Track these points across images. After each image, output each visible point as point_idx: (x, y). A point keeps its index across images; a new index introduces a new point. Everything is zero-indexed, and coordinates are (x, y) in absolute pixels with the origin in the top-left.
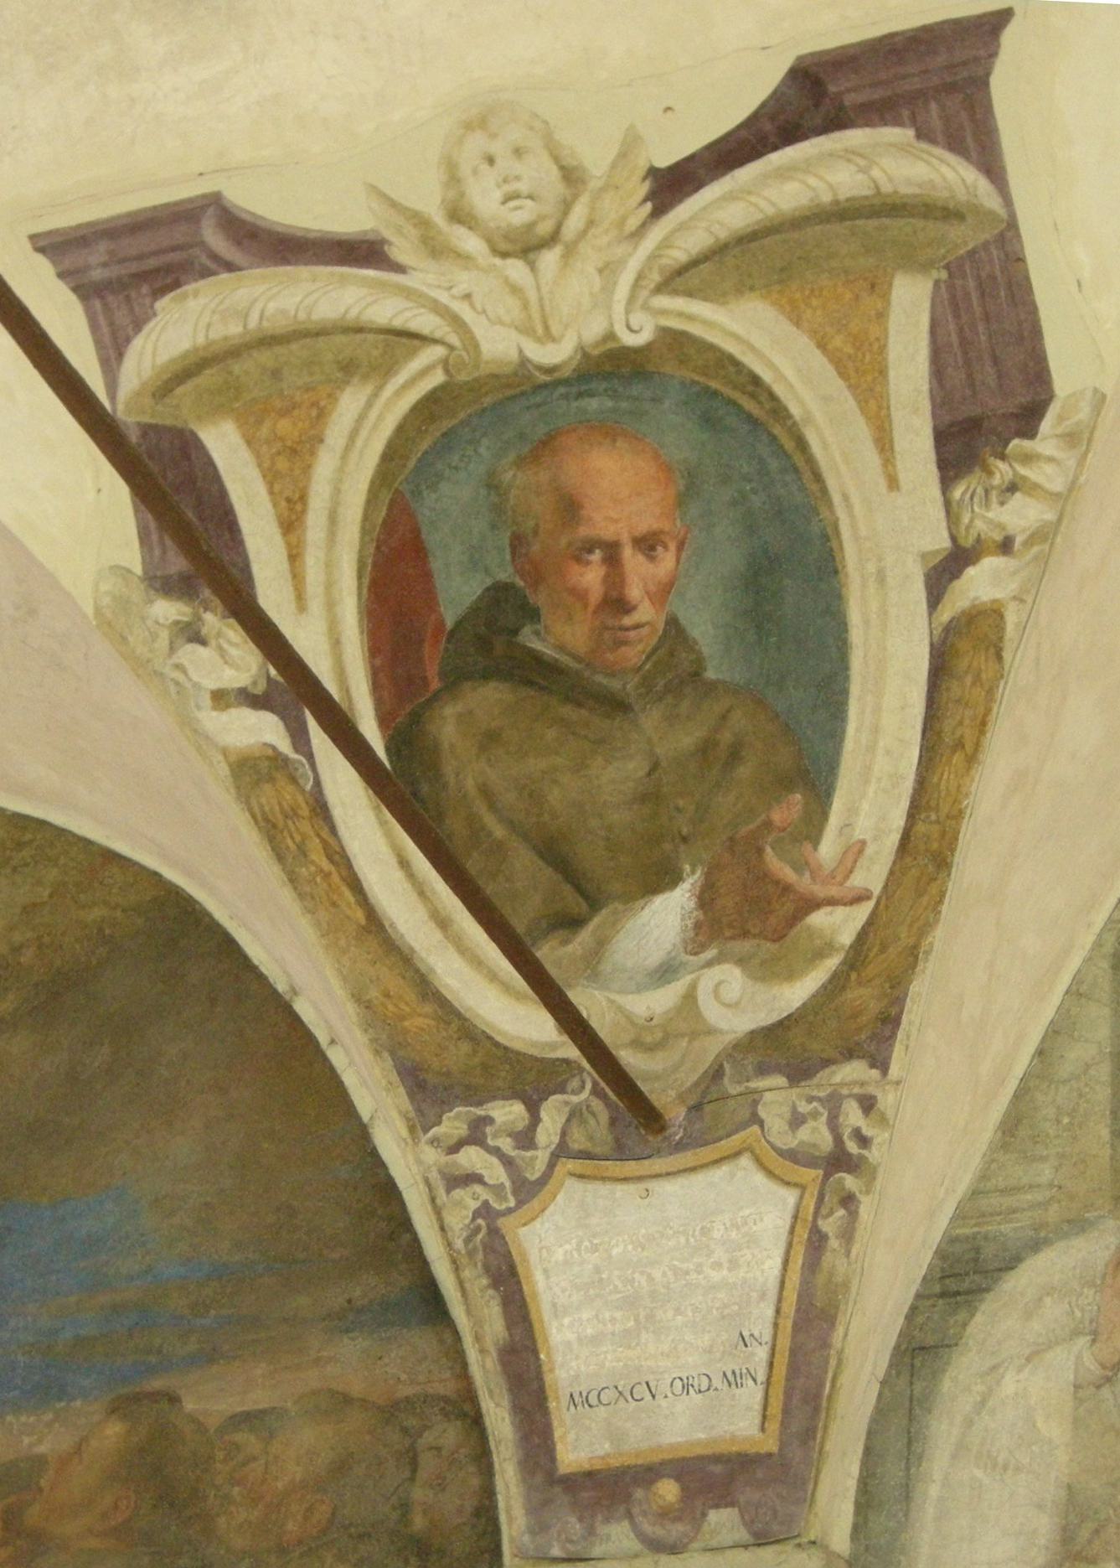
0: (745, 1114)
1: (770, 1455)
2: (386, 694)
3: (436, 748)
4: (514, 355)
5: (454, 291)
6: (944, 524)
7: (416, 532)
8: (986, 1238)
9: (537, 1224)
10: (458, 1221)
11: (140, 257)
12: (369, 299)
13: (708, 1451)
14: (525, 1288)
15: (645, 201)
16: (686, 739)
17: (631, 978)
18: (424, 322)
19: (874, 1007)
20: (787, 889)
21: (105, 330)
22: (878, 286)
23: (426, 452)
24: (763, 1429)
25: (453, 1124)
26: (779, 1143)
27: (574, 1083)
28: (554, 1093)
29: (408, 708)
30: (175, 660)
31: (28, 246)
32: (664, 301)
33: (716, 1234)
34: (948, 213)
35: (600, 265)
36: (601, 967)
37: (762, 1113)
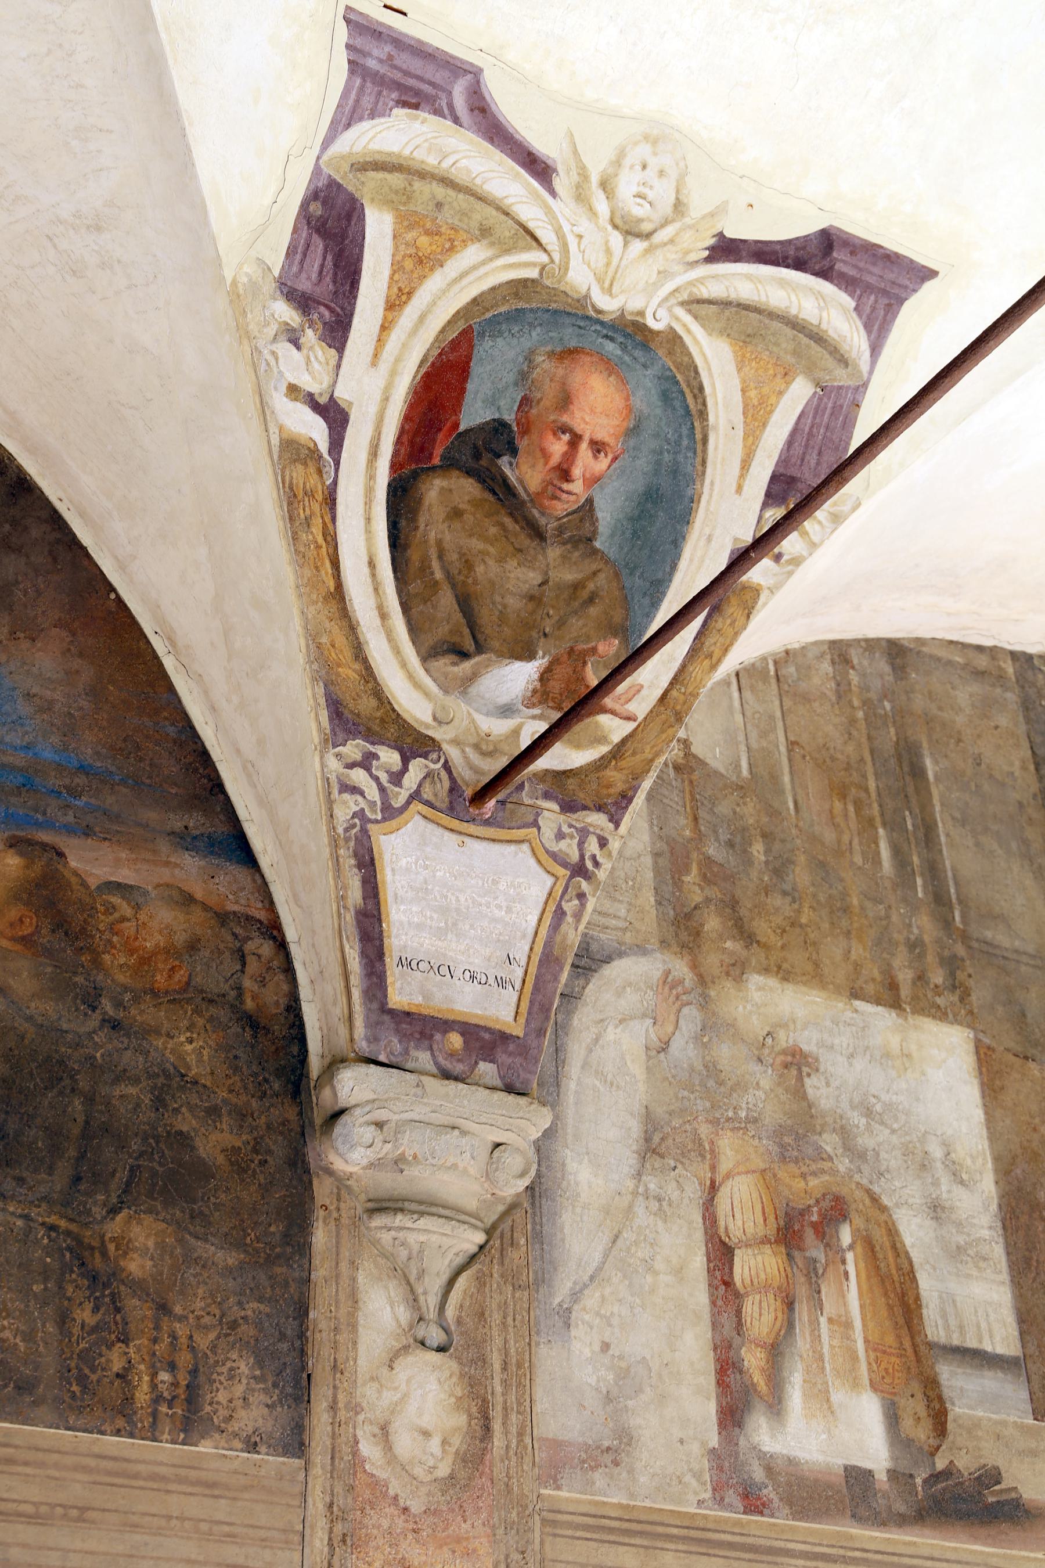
0: (531, 818)
1: (518, 1038)
2: (403, 451)
3: (419, 501)
4: (583, 290)
5: (575, 228)
6: (753, 528)
7: (469, 358)
8: (592, 938)
9: (393, 836)
11: (407, 73)
12: (524, 200)
13: (482, 1023)
14: (378, 876)
15: (706, 249)
16: (569, 576)
17: (485, 705)
18: (546, 235)
19: (620, 787)
21: (351, 102)
22: (788, 375)
23: (501, 314)
24: (515, 1020)
25: (353, 749)
26: (547, 845)
27: (435, 756)
28: (420, 757)
29: (413, 466)
30: (274, 347)
31: (341, 11)
32: (680, 312)
34: (843, 361)
35: (661, 269)
36: (470, 690)
37: (541, 822)
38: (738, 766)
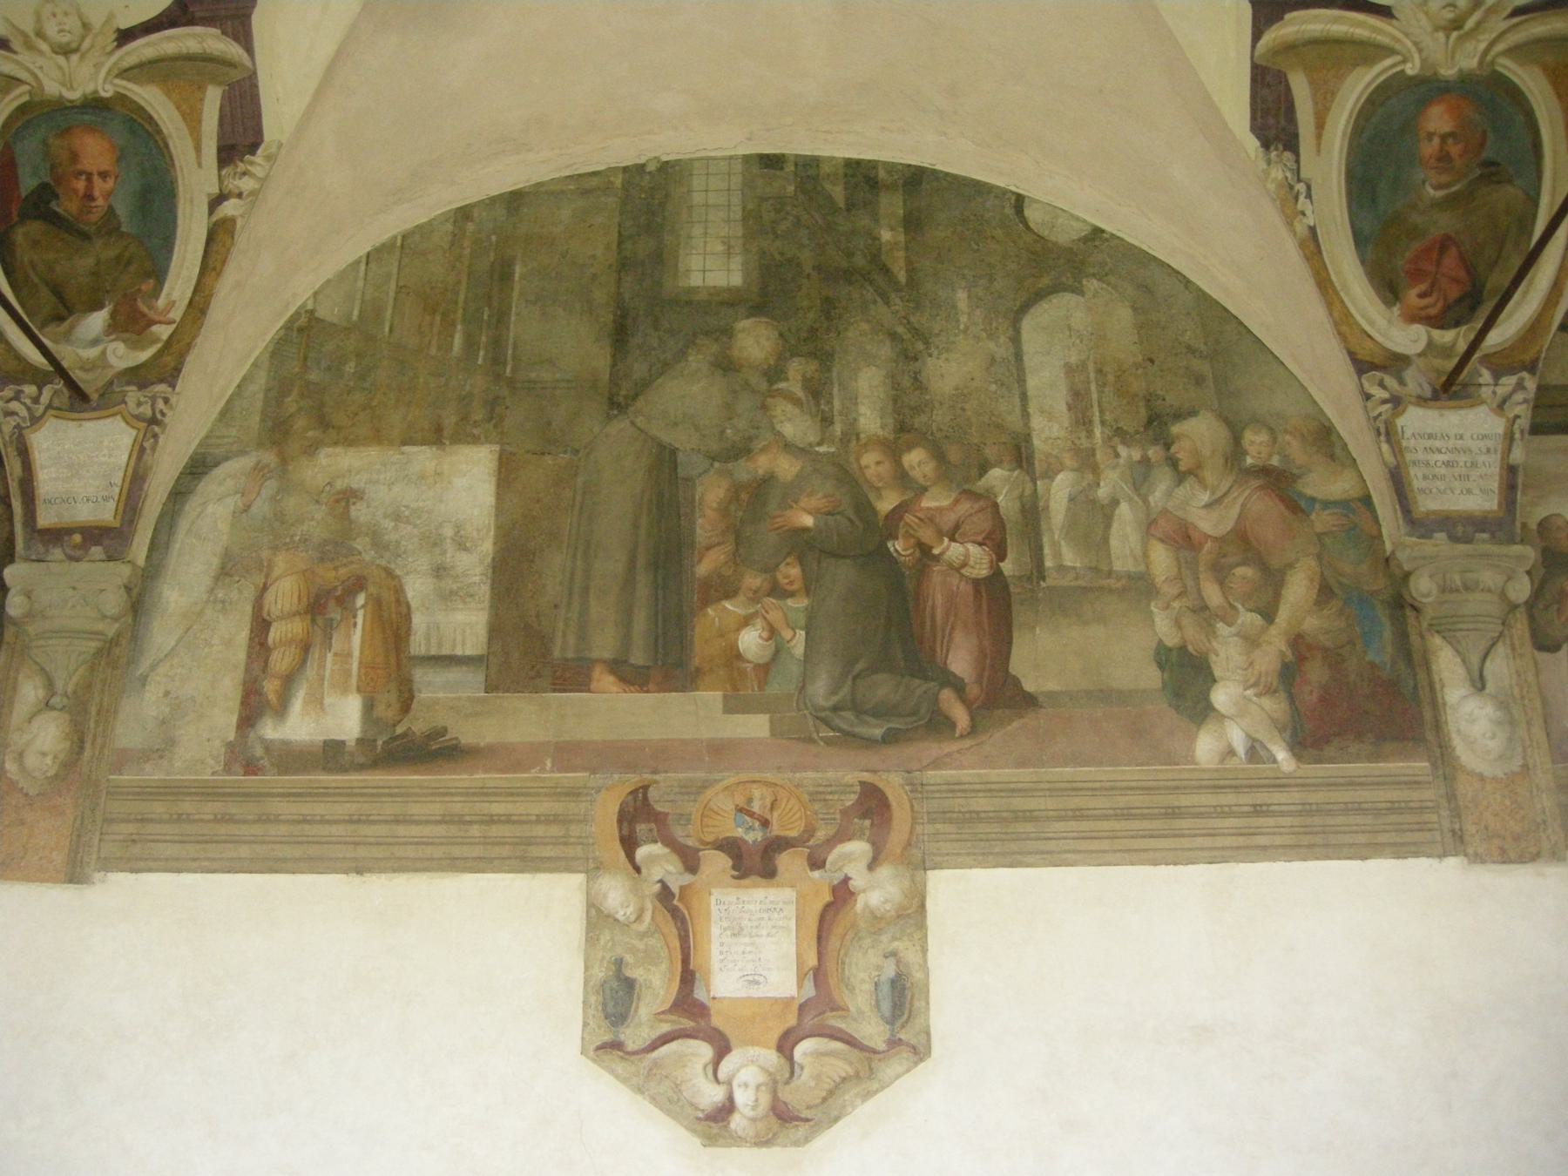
4: (58, 94)
10: (7, 429)
16: (111, 253)
18: (23, 75)
20: (144, 315)
22: (201, 88)
24: (115, 518)
26: (130, 410)
32: (118, 81)
33: (106, 443)
34: (231, 65)
37: (127, 399)
38: (351, 313)
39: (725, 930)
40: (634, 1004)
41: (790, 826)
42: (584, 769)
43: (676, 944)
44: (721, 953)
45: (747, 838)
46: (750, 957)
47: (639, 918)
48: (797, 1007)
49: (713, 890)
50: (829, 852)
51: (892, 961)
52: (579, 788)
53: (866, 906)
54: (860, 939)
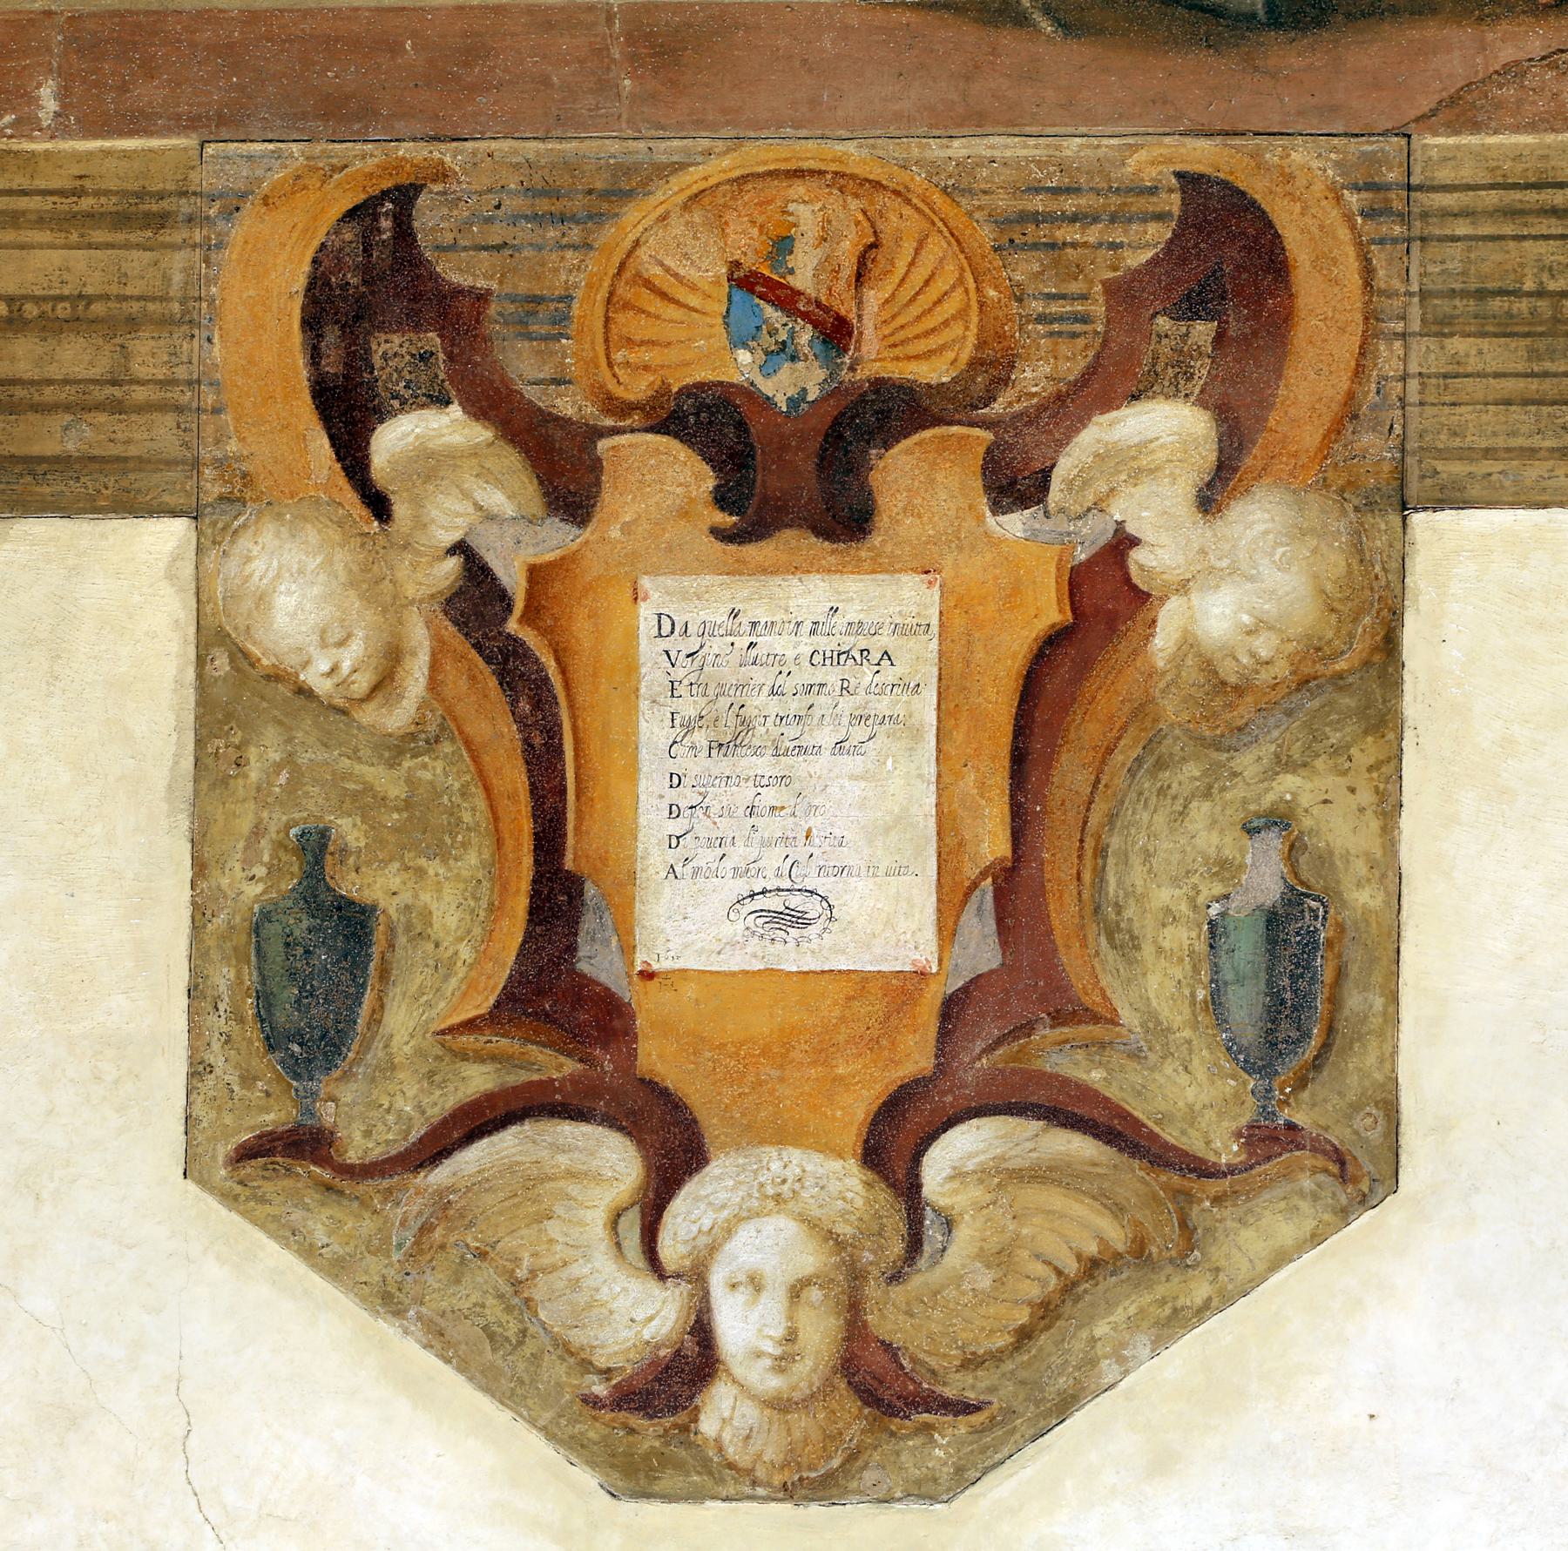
39: (689, 728)
40: (368, 998)
41: (921, 346)
42: (190, 124)
43: (514, 777)
44: (674, 811)
45: (767, 387)
46: (771, 826)
47: (384, 684)
48: (938, 1002)
49: (646, 582)
50: (1061, 444)
51: (1273, 841)
52: (161, 196)
53: (1188, 643)
54: (1160, 765)
